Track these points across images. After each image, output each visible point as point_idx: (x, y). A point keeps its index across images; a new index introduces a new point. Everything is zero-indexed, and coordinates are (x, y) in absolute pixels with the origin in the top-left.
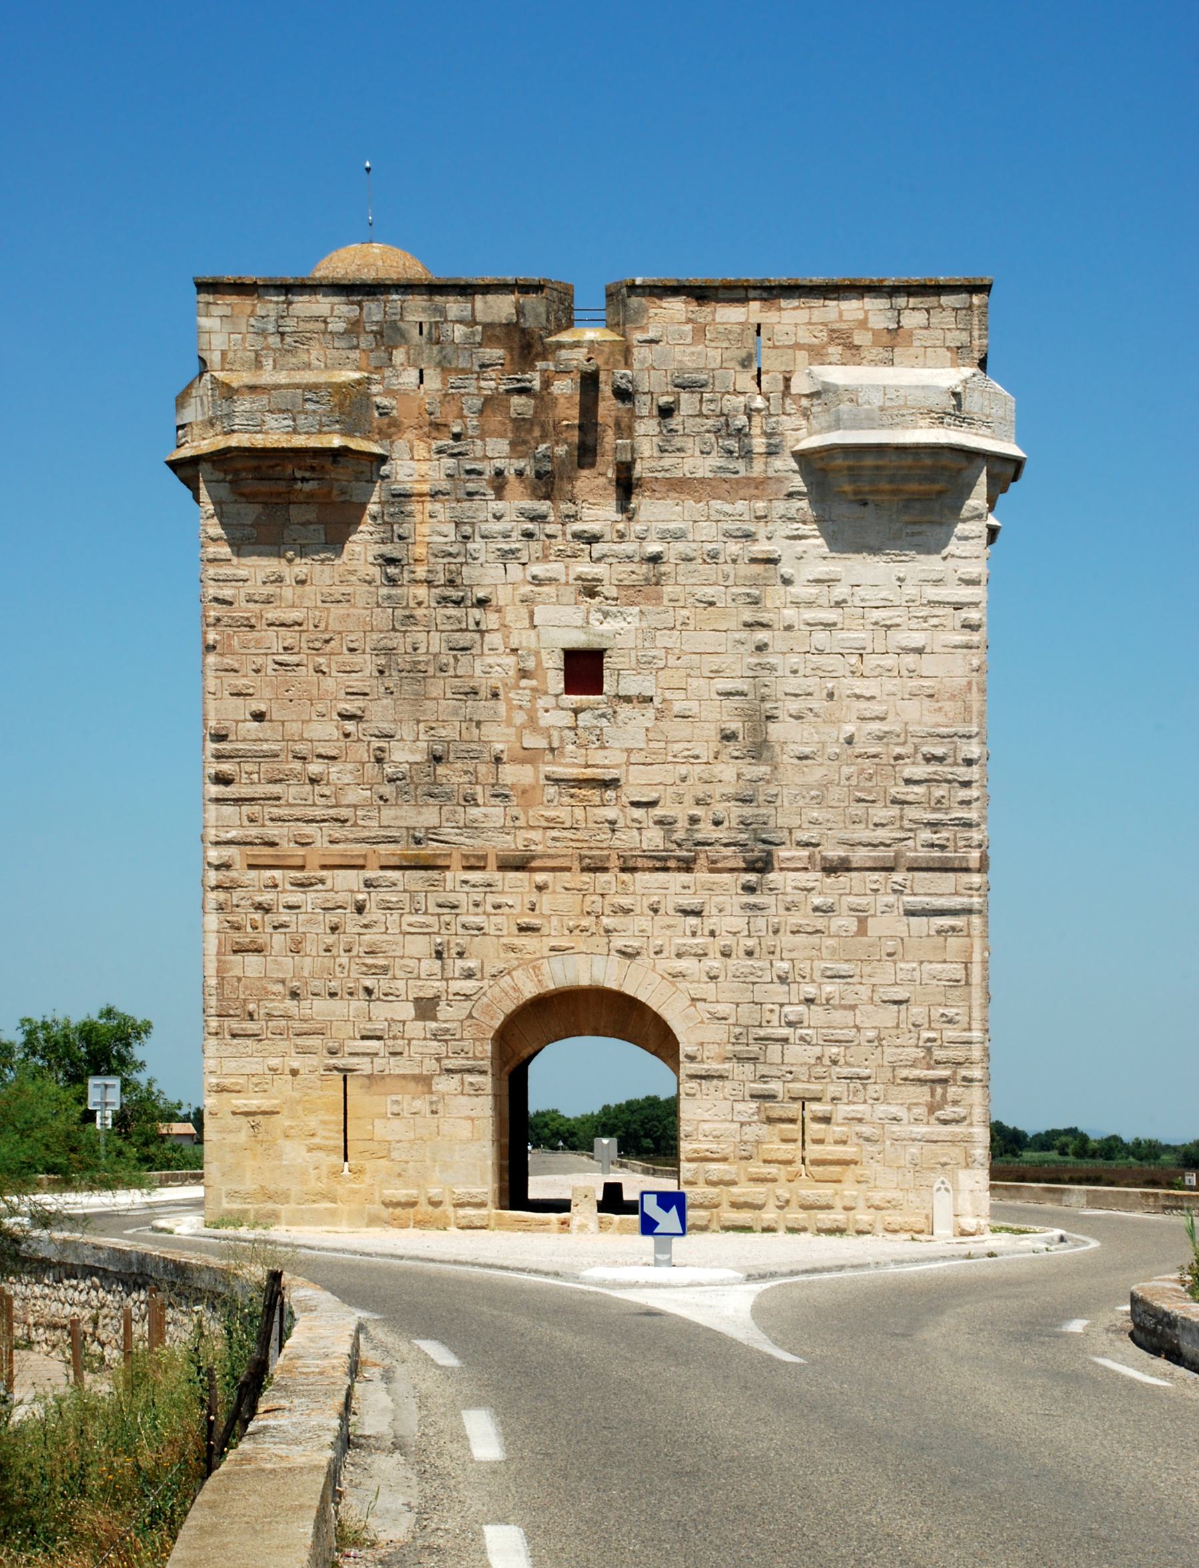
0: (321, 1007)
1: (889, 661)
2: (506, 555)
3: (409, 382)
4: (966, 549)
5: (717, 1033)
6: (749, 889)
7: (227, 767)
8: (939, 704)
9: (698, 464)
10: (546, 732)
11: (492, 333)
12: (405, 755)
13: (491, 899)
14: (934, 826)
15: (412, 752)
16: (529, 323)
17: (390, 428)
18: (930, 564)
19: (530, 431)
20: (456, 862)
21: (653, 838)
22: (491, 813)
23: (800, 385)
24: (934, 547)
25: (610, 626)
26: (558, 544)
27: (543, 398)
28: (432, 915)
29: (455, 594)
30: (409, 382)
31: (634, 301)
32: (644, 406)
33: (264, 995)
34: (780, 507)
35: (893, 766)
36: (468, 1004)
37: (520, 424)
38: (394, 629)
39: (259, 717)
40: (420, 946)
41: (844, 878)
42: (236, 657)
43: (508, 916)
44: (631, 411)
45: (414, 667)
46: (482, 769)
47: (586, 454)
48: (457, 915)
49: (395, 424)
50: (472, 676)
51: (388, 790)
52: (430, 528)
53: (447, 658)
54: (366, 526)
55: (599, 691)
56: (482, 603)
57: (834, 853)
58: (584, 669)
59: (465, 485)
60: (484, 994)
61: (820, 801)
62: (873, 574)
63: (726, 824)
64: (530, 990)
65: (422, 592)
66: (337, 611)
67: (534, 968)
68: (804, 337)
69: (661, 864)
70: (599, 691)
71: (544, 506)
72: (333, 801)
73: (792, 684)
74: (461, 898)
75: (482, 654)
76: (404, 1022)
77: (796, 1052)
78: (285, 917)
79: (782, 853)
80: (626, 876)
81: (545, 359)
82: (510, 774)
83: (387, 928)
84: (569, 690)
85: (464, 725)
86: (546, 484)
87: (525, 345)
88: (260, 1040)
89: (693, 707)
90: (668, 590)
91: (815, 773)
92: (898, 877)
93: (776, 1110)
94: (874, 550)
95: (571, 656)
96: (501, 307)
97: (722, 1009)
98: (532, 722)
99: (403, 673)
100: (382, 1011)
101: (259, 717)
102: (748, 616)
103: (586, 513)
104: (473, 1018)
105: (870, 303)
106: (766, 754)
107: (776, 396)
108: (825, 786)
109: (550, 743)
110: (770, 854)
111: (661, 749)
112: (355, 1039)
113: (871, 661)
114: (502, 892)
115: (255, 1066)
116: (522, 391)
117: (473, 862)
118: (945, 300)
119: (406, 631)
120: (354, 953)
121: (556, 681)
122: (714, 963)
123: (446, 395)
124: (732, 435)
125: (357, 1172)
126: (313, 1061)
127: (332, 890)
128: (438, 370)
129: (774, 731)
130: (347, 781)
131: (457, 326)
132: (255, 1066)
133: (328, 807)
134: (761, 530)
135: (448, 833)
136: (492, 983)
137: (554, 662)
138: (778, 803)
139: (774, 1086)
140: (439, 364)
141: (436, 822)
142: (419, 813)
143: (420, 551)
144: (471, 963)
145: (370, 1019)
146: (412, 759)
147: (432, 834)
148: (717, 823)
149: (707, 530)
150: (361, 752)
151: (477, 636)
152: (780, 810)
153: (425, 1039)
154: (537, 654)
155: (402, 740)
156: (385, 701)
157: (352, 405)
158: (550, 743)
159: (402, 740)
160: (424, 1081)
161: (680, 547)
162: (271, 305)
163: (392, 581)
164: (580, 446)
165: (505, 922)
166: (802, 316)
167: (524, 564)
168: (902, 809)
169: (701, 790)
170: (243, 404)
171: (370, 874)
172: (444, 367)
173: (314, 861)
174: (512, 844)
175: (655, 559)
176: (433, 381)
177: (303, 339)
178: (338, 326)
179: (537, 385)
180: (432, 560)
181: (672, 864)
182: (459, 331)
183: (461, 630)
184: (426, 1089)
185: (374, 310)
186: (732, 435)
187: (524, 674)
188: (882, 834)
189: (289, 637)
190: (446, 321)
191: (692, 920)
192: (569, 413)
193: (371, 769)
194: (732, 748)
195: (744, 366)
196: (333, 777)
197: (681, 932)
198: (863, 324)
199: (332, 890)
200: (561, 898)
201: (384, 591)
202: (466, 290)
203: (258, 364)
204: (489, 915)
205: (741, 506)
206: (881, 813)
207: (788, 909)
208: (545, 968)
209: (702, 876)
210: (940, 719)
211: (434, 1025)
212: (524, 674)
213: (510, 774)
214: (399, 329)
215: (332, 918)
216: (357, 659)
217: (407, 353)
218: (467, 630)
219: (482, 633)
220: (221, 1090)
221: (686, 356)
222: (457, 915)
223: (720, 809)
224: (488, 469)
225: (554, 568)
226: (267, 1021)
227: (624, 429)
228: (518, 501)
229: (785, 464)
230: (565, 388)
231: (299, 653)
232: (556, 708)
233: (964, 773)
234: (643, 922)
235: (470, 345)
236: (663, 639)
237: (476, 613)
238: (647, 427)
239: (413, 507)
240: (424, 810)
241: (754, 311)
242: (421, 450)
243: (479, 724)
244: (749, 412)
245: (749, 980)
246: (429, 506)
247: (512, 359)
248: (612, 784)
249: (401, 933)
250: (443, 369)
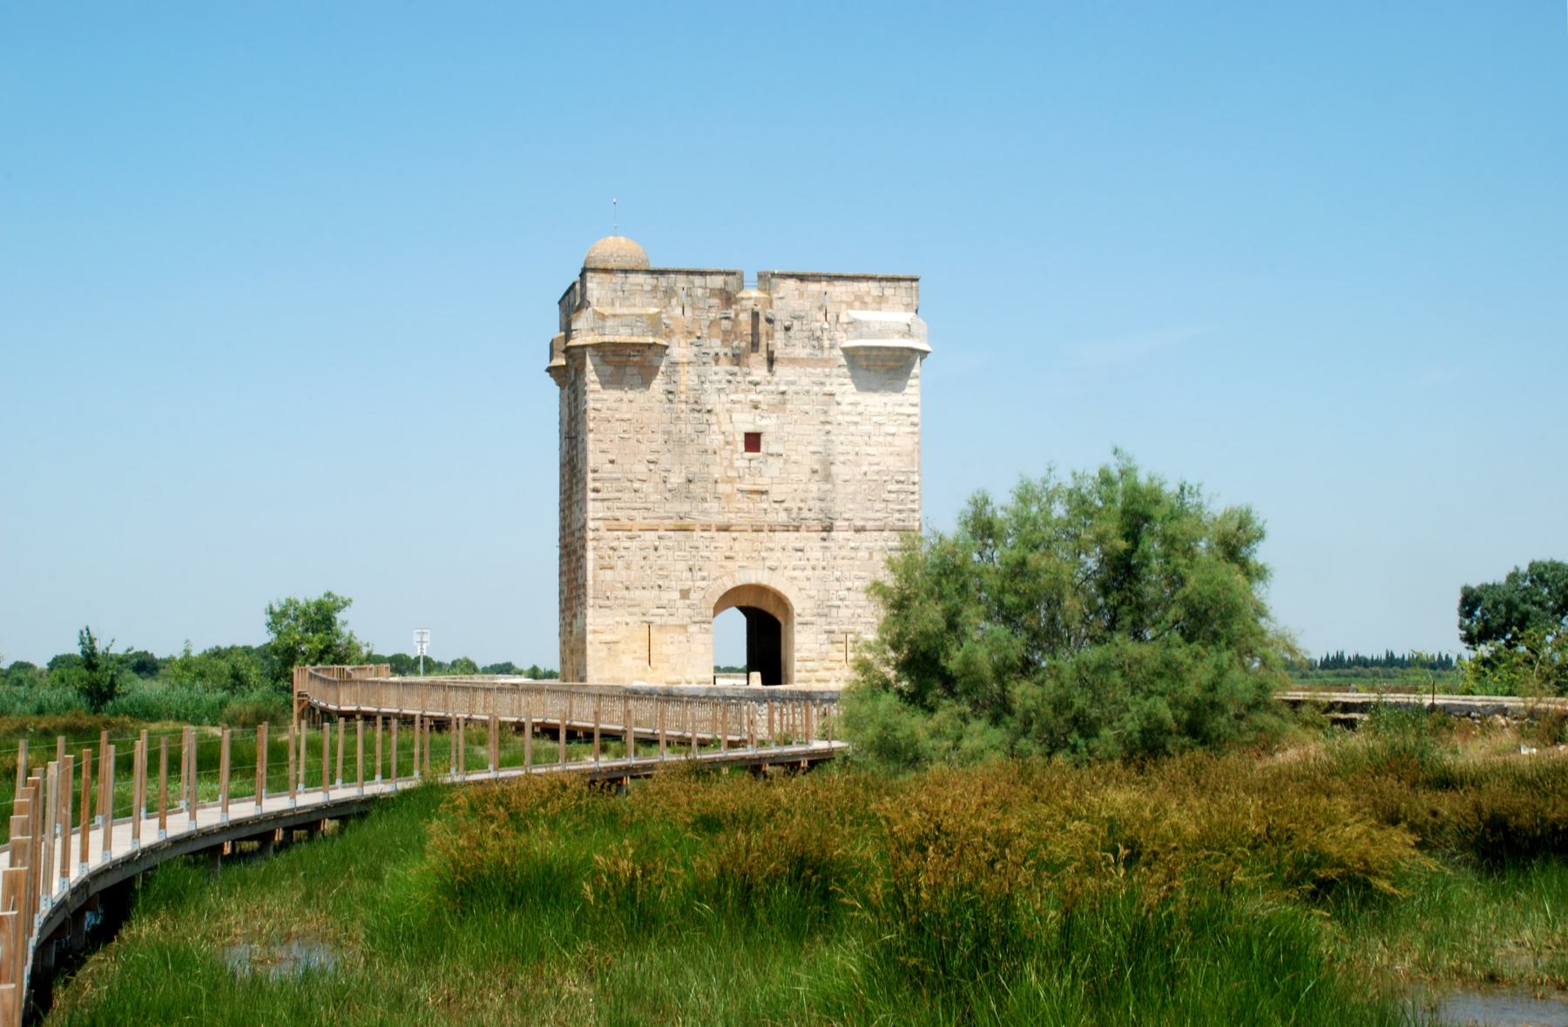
0: (637, 594)
1: (881, 439)
2: (719, 390)
3: (675, 313)
4: (913, 389)
5: (810, 604)
6: (824, 539)
7: (597, 485)
9: (802, 352)
10: (737, 469)
11: (714, 293)
12: (676, 479)
14: (900, 511)
16: (729, 289)
17: (670, 333)
18: (897, 397)
20: (698, 528)
21: (782, 517)
22: (713, 506)
23: (843, 319)
24: (899, 390)
25: (764, 422)
26: (742, 386)
27: (735, 321)
29: (698, 407)
30: (675, 313)
31: (774, 280)
32: (778, 326)
33: (613, 588)
34: (835, 371)
37: (726, 333)
39: (612, 462)
40: (682, 566)
41: (863, 534)
45: (680, 440)
47: (755, 346)
49: (672, 331)
51: (668, 495)
52: (687, 378)
53: (694, 436)
54: (660, 376)
55: (758, 450)
56: (709, 411)
57: (859, 523)
58: (753, 441)
59: (704, 359)
61: (853, 500)
62: (876, 402)
64: (730, 586)
65: (683, 406)
66: (646, 414)
68: (844, 298)
70: (758, 450)
71: (736, 369)
73: (842, 449)
74: (700, 544)
77: (844, 613)
78: (623, 553)
79: (837, 523)
82: (721, 488)
86: (737, 359)
87: (728, 298)
89: (799, 458)
90: (789, 406)
91: (851, 488)
92: (885, 534)
93: (835, 637)
94: (875, 391)
95: (747, 435)
96: (718, 282)
97: (813, 593)
98: (731, 464)
99: (675, 443)
100: (665, 596)
101: (612, 462)
102: (822, 418)
103: (754, 371)
105: (872, 285)
108: (855, 493)
111: (785, 476)
113: (874, 439)
115: (610, 621)
118: (902, 284)
121: (741, 447)
122: (809, 573)
124: (815, 339)
125: (655, 669)
126: (635, 618)
129: (834, 469)
132: (610, 621)
134: (828, 381)
135: (695, 514)
137: (741, 439)
139: (834, 627)
143: (682, 388)
144: (705, 574)
147: (687, 515)
149: (805, 380)
150: (657, 478)
157: (655, 323)
160: (684, 627)
161: (794, 388)
162: (620, 277)
163: (670, 401)
164: (753, 343)
165: (719, 555)
166: (843, 289)
169: (803, 496)
170: (610, 323)
171: (661, 533)
172: (693, 307)
173: (636, 527)
174: (722, 519)
175: (783, 393)
177: (632, 293)
178: (647, 288)
182: (700, 292)
185: (663, 281)
186: (815, 339)
187: (727, 443)
188: (878, 515)
189: (625, 426)
192: (747, 329)
193: (661, 486)
194: (816, 477)
197: (795, 559)
198: (868, 293)
200: (743, 544)
202: (702, 273)
203: (613, 304)
205: (819, 370)
206: (878, 506)
209: (803, 534)
212: (727, 443)
213: (721, 488)
215: (644, 553)
216: (655, 436)
220: (595, 632)
223: (811, 503)
225: (740, 396)
227: (770, 336)
228: (725, 366)
229: (838, 353)
230: (745, 317)
232: (742, 458)
233: (912, 488)
234: (779, 554)
235: (706, 298)
236: (787, 428)
237: (707, 416)
238: (779, 335)
239: (679, 368)
241: (823, 286)
242: (683, 343)
244: (822, 330)
245: (823, 580)
246: (687, 368)
248: (763, 493)
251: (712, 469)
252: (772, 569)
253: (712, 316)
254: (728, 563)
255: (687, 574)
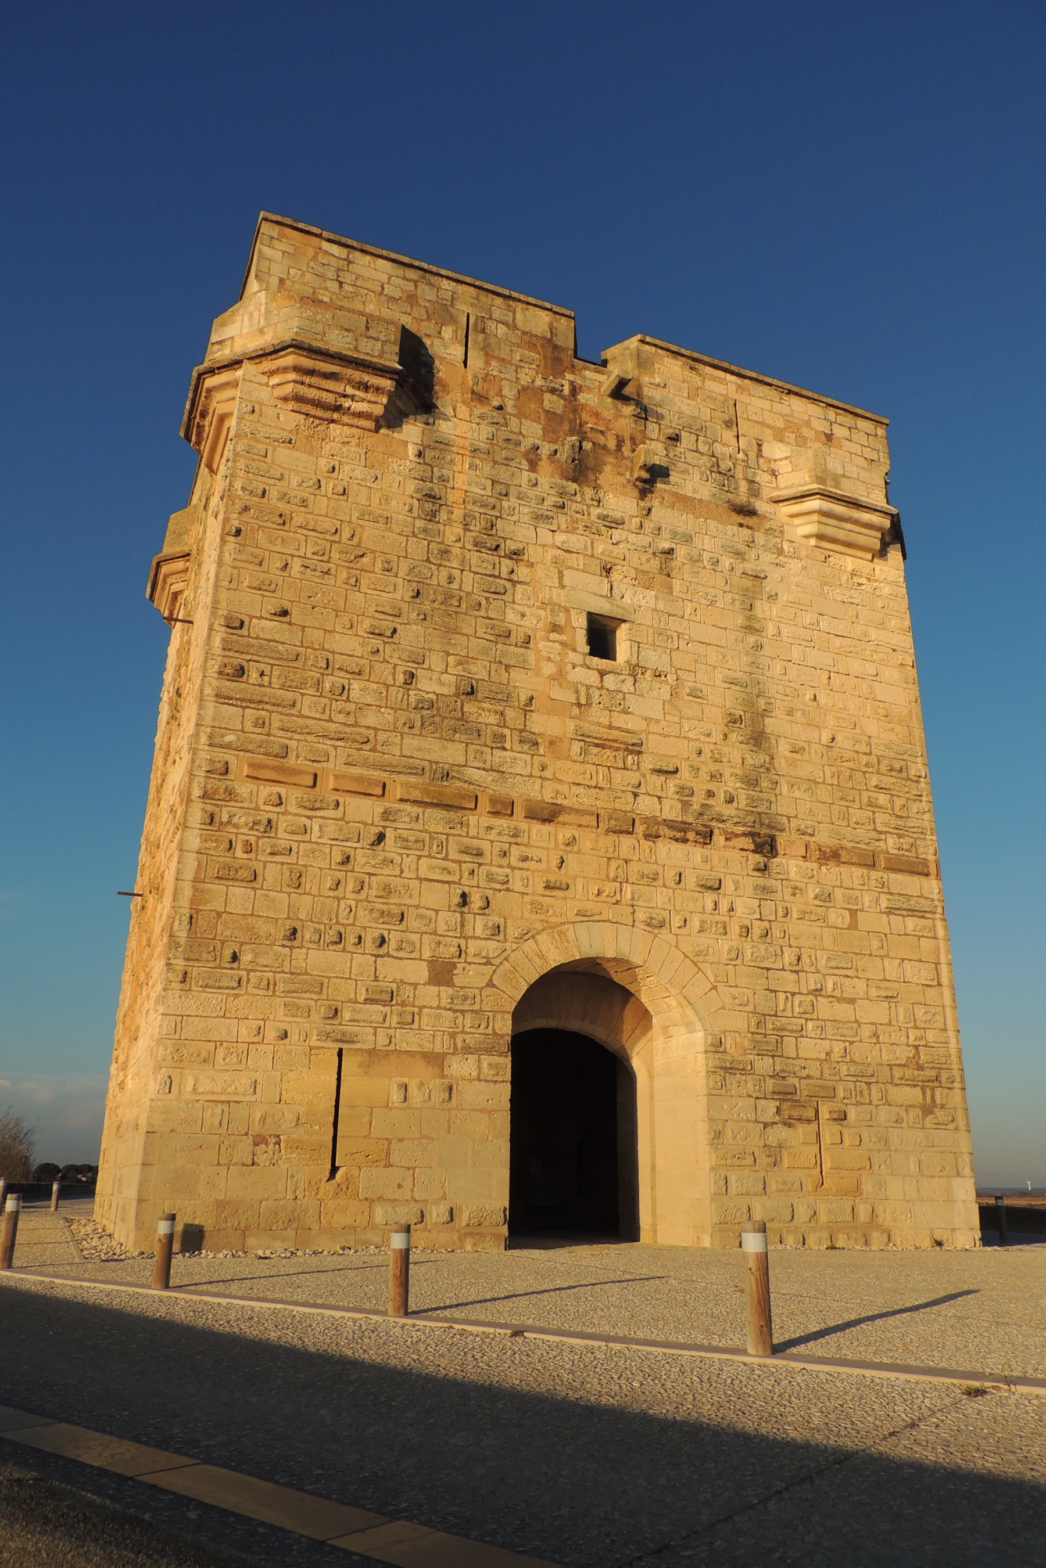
0: (314, 959)
8: (890, 726)
11: (530, 340)
13: (515, 851)
15: (442, 684)
19: (561, 423)
20: (484, 805)
21: (671, 810)
22: (517, 760)
28: (453, 861)
35: (865, 773)
36: (489, 969)
37: (550, 415)
38: (428, 560)
40: (437, 897)
42: (257, 551)
43: (534, 871)
44: (644, 432)
46: (510, 713)
48: (480, 865)
50: (503, 621)
56: (516, 555)
60: (506, 959)
63: (735, 804)
67: (560, 933)
69: (680, 832)
72: (351, 720)
75: (514, 602)
76: (415, 985)
79: (781, 841)
80: (646, 844)
81: (573, 373)
82: (538, 723)
83: (402, 872)
84: (592, 653)
85: (494, 666)
88: (236, 996)
98: (559, 676)
100: (391, 970)
104: (494, 986)
106: (765, 745)
107: (753, 455)
109: (578, 699)
110: (773, 838)
112: (356, 1002)
114: (527, 845)
116: (553, 391)
117: (499, 807)
119: (440, 565)
120: (363, 895)
123: (487, 375)
127: (342, 819)
128: (482, 353)
130: (369, 702)
131: (500, 325)
133: (345, 724)
136: (515, 946)
137: (581, 622)
138: (778, 791)
140: (483, 349)
141: (461, 760)
142: (445, 748)
145: (376, 979)
146: (440, 690)
148: (730, 800)
151: (508, 585)
152: (779, 797)
153: (439, 1007)
154: (567, 611)
155: (429, 669)
156: (414, 627)
158: (578, 699)
159: (429, 669)
166: (767, 405)
167: (553, 531)
168: (874, 812)
175: (670, 552)
176: (476, 360)
179: (566, 390)
180: (470, 507)
181: (691, 836)
183: (494, 576)
184: (437, 1070)
187: (555, 628)
190: (491, 318)
191: (709, 898)
195: (728, 427)
196: (355, 694)
199: (342, 819)
201: (420, 523)
204: (513, 868)
206: (856, 814)
207: (794, 895)
208: (571, 934)
210: (892, 737)
211: (450, 991)
212: (555, 628)
214: (449, 312)
217: (455, 332)
218: (499, 577)
219: (515, 583)
221: (686, 407)
222: (480, 865)
224: (527, 444)
226: (249, 971)
228: (547, 479)
231: (328, 562)
232: (584, 670)
237: (506, 564)
240: (450, 744)
242: (463, 411)
243: (507, 667)
247: (546, 364)
248: (635, 749)
249: (417, 878)
250: (487, 355)
251: (517, 677)
252: (656, 924)
253: (525, 380)
254: (555, 902)
255: (447, 919)
